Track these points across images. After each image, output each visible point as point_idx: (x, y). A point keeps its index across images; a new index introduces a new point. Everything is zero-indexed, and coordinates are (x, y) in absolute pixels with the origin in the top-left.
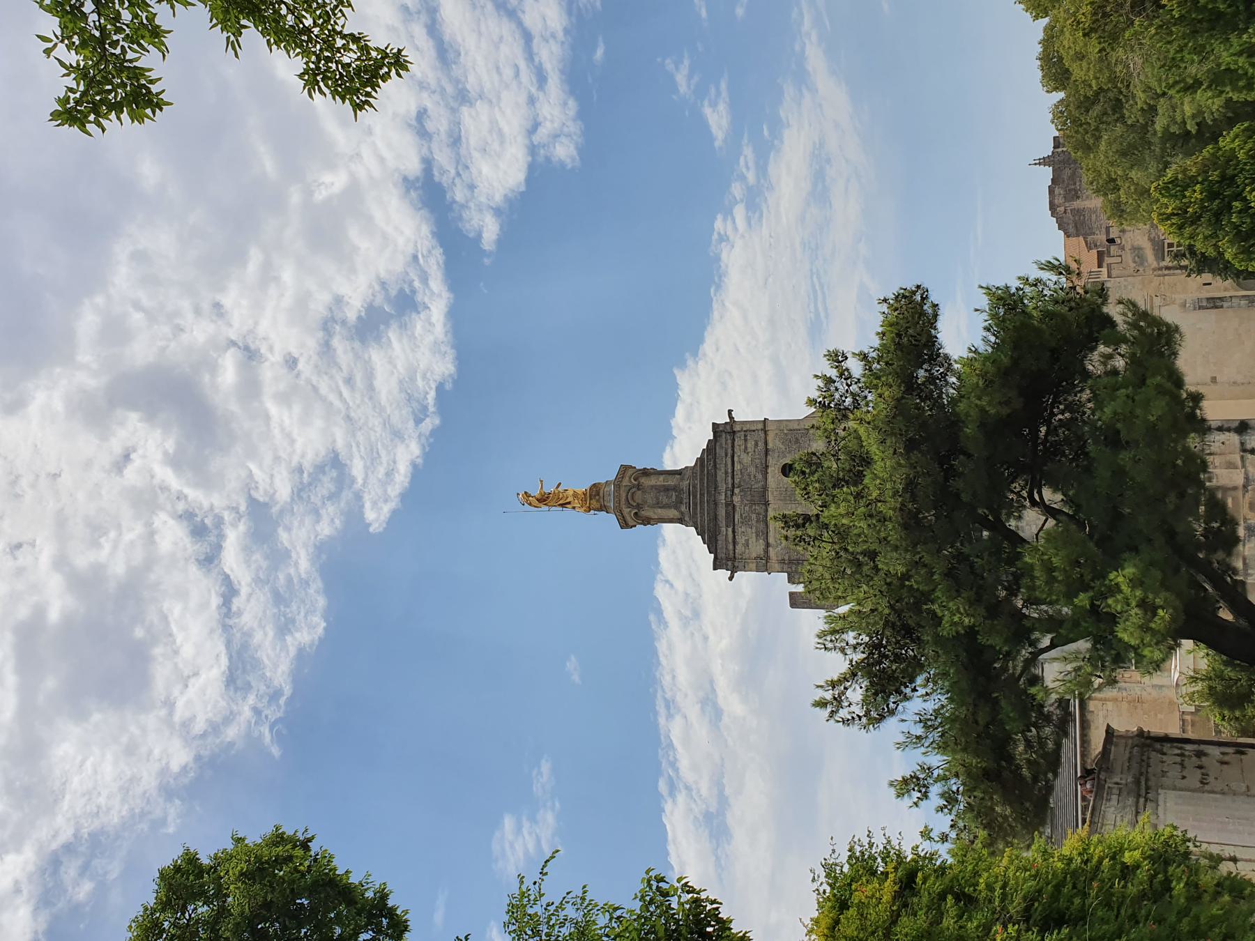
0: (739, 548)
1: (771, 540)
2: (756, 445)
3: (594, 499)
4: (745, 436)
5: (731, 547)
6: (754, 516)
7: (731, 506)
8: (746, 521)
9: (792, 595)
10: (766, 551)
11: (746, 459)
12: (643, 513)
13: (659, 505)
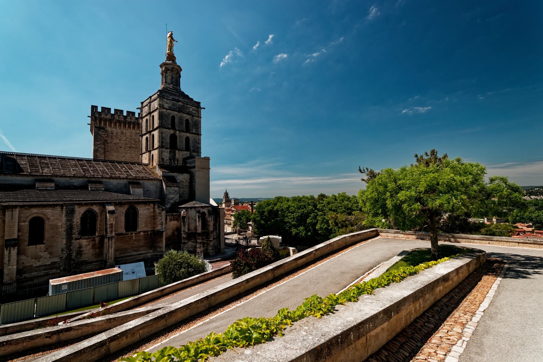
0: (165, 100)
1: (168, 111)
2: (194, 113)
3: (171, 57)
4: (197, 111)
5: (166, 97)
6: (175, 107)
7: (178, 101)
8: (174, 105)
9: (96, 107)
10: (165, 108)
11: (191, 110)
12: (169, 72)
13: (172, 78)
